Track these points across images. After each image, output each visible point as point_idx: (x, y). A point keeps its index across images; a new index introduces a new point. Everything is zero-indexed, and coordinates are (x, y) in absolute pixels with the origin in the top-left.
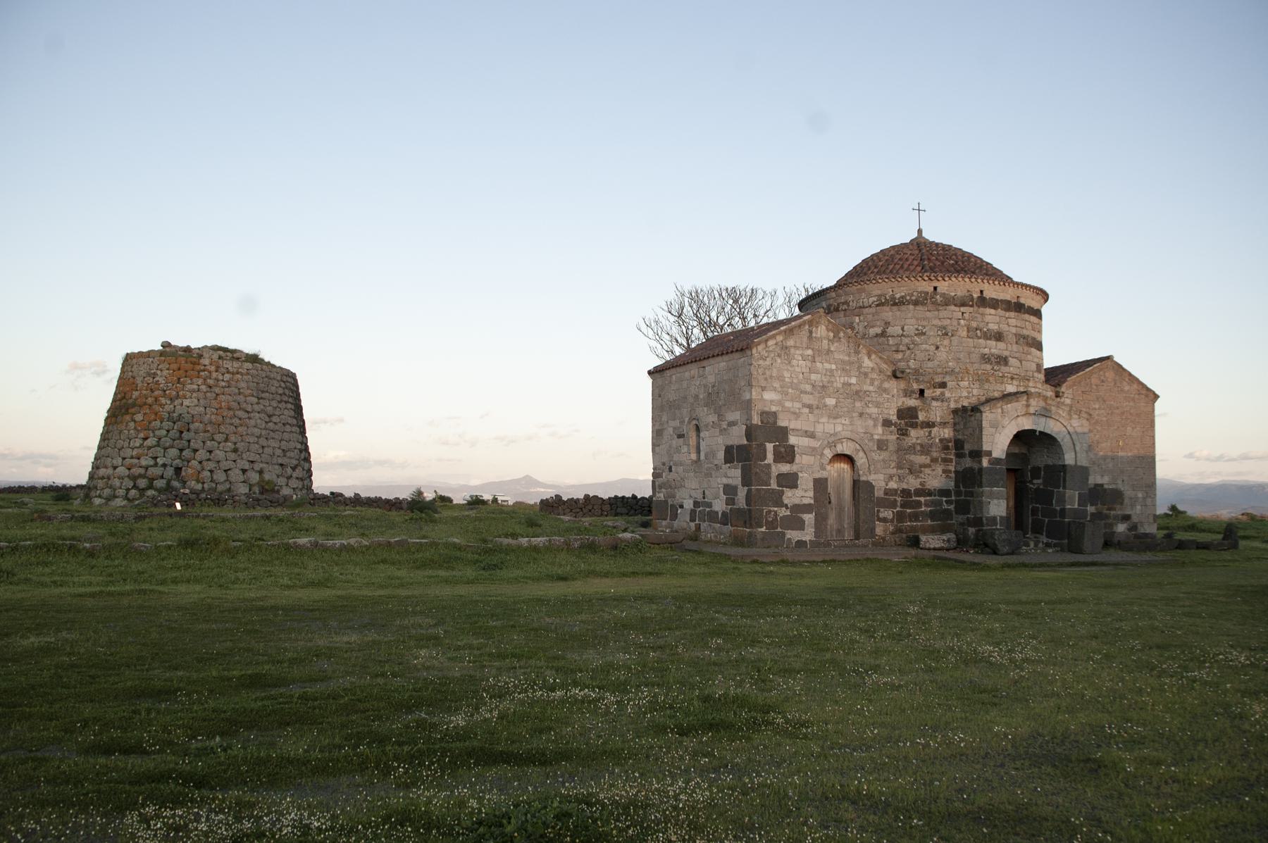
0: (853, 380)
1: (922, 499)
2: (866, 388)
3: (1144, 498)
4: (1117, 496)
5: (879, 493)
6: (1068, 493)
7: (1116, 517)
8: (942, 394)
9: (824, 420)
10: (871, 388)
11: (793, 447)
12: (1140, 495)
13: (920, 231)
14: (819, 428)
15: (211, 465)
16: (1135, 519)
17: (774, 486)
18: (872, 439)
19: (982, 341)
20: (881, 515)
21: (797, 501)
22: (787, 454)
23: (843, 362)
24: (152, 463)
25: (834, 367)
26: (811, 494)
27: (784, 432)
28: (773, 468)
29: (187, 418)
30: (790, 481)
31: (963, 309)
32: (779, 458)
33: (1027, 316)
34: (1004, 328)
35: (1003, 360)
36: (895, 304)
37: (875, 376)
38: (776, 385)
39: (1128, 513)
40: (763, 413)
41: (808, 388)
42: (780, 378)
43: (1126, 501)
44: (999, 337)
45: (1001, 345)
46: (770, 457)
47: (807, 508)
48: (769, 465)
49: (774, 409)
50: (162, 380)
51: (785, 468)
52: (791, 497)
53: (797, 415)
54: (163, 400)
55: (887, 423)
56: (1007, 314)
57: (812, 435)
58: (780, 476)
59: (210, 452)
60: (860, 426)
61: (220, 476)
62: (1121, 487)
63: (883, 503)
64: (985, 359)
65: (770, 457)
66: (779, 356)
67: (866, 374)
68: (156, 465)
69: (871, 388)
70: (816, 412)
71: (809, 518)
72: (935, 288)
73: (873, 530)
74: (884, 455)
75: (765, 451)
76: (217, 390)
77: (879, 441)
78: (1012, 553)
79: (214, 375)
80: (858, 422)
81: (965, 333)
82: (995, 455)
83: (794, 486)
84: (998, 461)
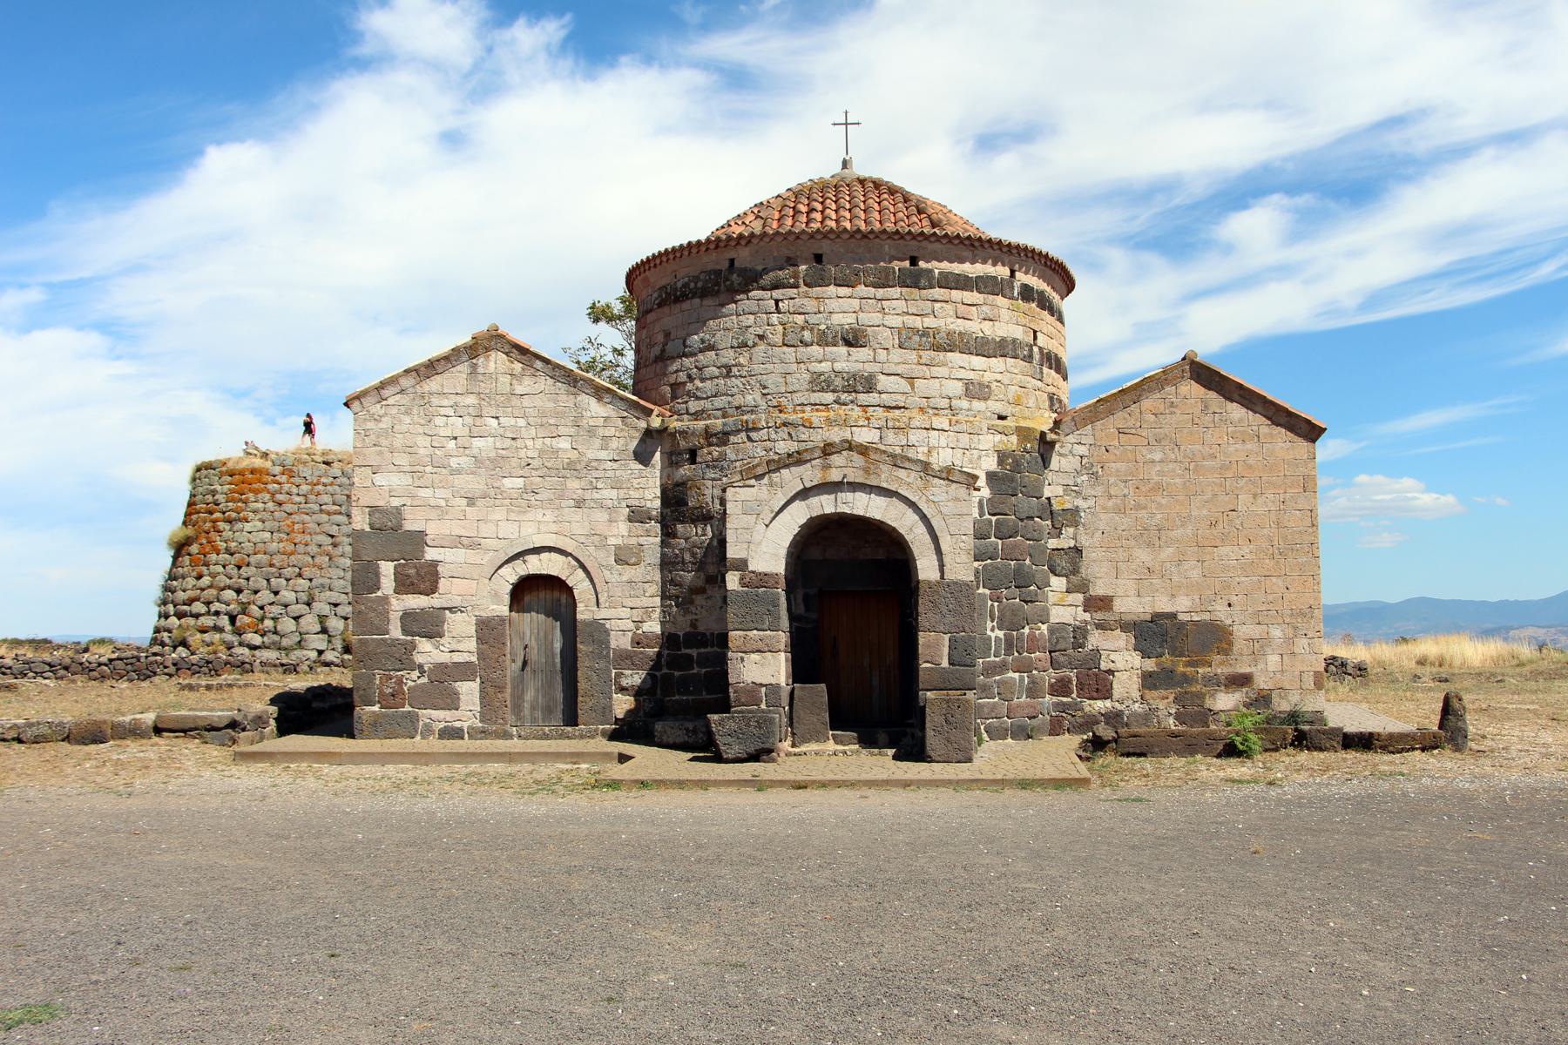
0: (564, 444)
1: (694, 652)
2: (590, 455)
3: (1290, 641)
4: (1215, 637)
5: (620, 641)
6: (923, 638)
7: (1215, 682)
8: (723, 457)
9: (499, 514)
10: (603, 455)
11: (434, 564)
12: (1276, 632)
13: (845, 164)
14: (487, 530)
15: (276, 610)
16: (1262, 682)
17: (396, 632)
18: (603, 546)
19: (816, 350)
20: (624, 682)
21: (445, 658)
22: (422, 578)
23: (542, 414)
24: (203, 609)
25: (522, 422)
26: (472, 645)
27: (419, 539)
28: (393, 601)
29: (248, 547)
30: (427, 625)
31: (777, 294)
32: (405, 585)
33: (937, 293)
34: (870, 318)
35: (869, 384)
36: (677, 300)
37: (610, 432)
38: (402, 459)
39: (1244, 669)
40: (374, 510)
41: (465, 461)
42: (410, 450)
43: (1239, 645)
44: (853, 339)
45: (861, 353)
46: (388, 583)
47: (463, 671)
48: (385, 599)
49: (396, 502)
50: (221, 498)
51: (416, 602)
52: (428, 652)
53: (442, 512)
54: (221, 525)
55: (637, 516)
56: (880, 293)
57: (474, 545)
58: (408, 618)
59: (276, 593)
60: (578, 523)
61: (287, 625)
62: (1221, 613)
63: (625, 659)
64: (820, 383)
65: (388, 583)
66: (407, 413)
67: (591, 432)
68: (208, 613)
69: (603, 455)
70: (480, 502)
71: (469, 691)
72: (732, 261)
73: (608, 708)
74: (629, 573)
75: (377, 575)
76: (288, 507)
77: (618, 548)
78: (754, 757)
79: (286, 487)
80: (576, 516)
81: (778, 339)
82: (757, 565)
83: (434, 634)
84: (764, 579)
